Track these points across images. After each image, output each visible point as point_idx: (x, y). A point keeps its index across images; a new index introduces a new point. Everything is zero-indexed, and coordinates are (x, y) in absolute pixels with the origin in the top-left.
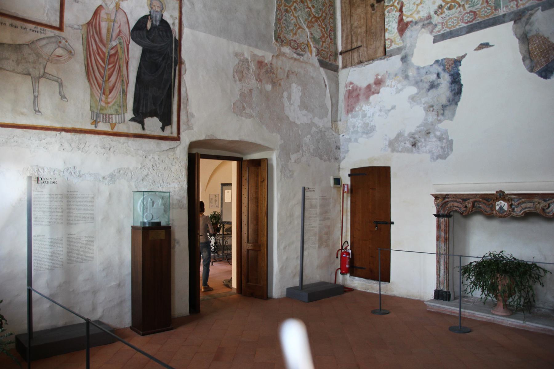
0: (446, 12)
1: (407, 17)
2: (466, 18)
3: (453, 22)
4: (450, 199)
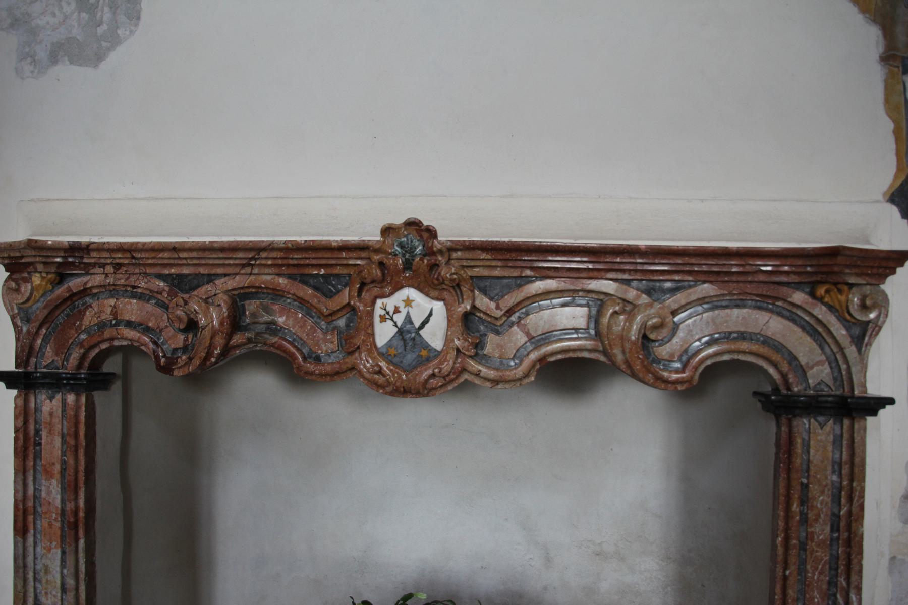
4: (96, 279)
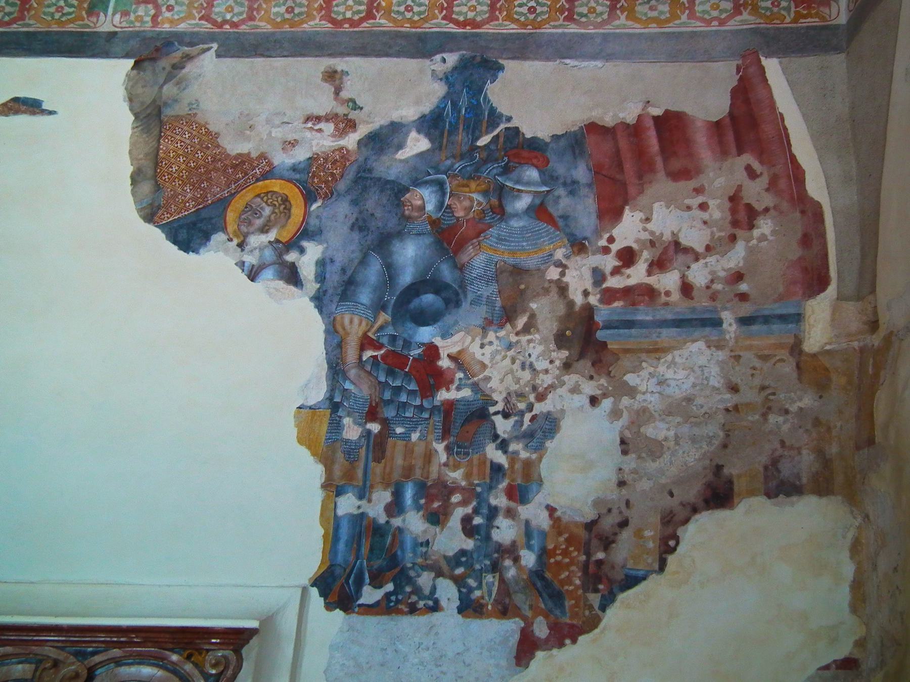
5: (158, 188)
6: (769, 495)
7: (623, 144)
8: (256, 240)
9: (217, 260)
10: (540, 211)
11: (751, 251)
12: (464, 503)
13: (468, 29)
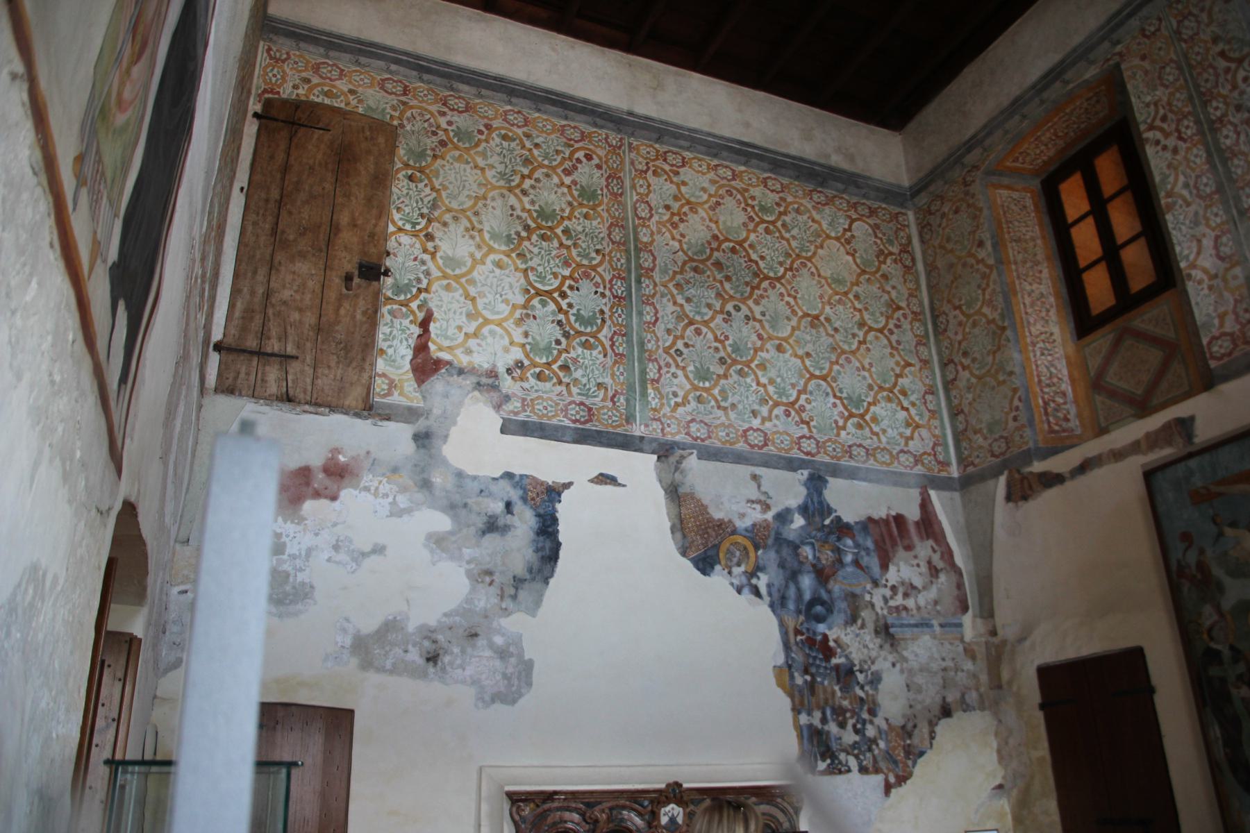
0: (533, 381)
1: (440, 349)
2: (573, 412)
3: (545, 408)
5: (684, 536)
6: (965, 711)
7: (884, 529)
8: (737, 570)
9: (719, 580)
10: (856, 563)
11: (939, 590)
12: (852, 717)
13: (809, 457)
